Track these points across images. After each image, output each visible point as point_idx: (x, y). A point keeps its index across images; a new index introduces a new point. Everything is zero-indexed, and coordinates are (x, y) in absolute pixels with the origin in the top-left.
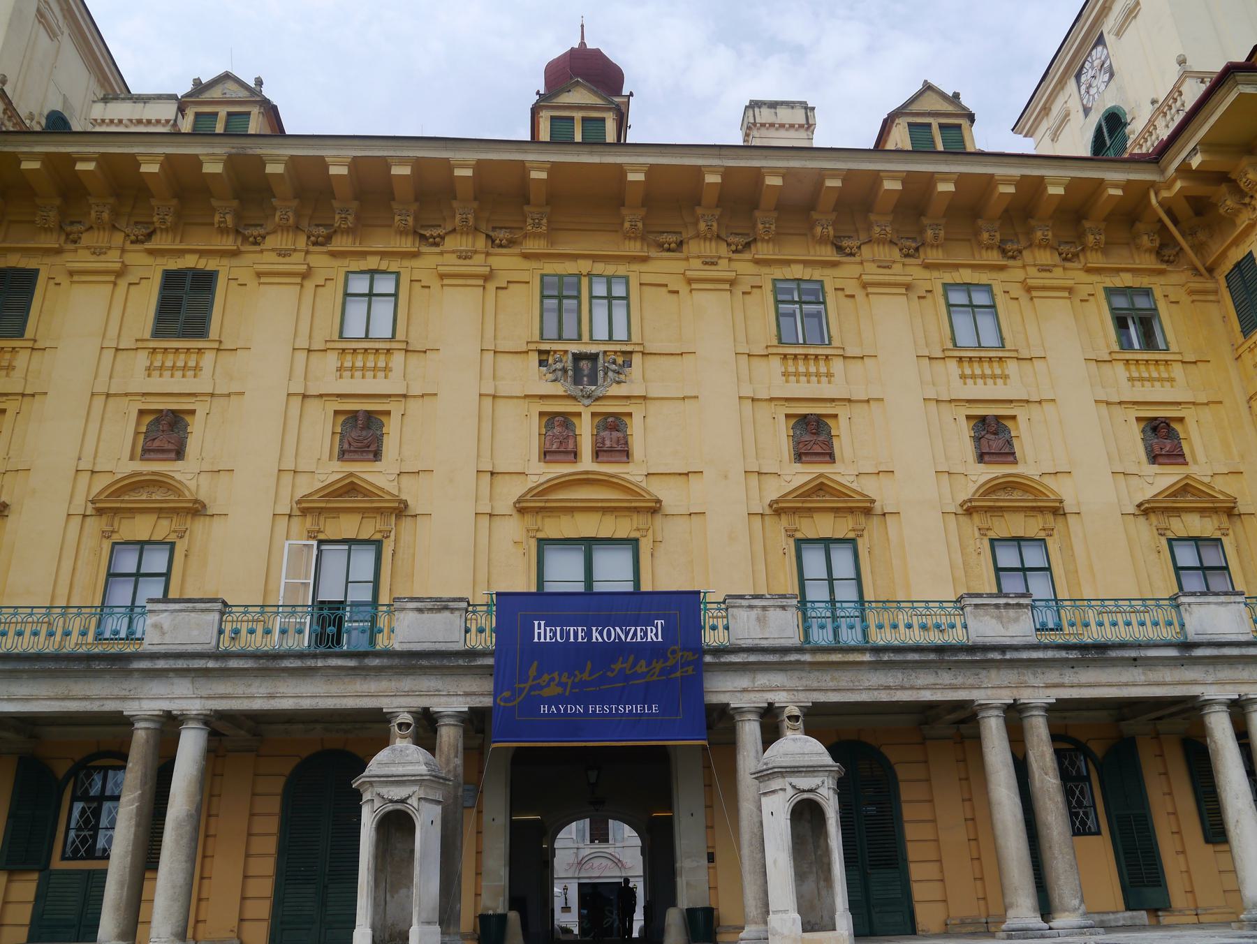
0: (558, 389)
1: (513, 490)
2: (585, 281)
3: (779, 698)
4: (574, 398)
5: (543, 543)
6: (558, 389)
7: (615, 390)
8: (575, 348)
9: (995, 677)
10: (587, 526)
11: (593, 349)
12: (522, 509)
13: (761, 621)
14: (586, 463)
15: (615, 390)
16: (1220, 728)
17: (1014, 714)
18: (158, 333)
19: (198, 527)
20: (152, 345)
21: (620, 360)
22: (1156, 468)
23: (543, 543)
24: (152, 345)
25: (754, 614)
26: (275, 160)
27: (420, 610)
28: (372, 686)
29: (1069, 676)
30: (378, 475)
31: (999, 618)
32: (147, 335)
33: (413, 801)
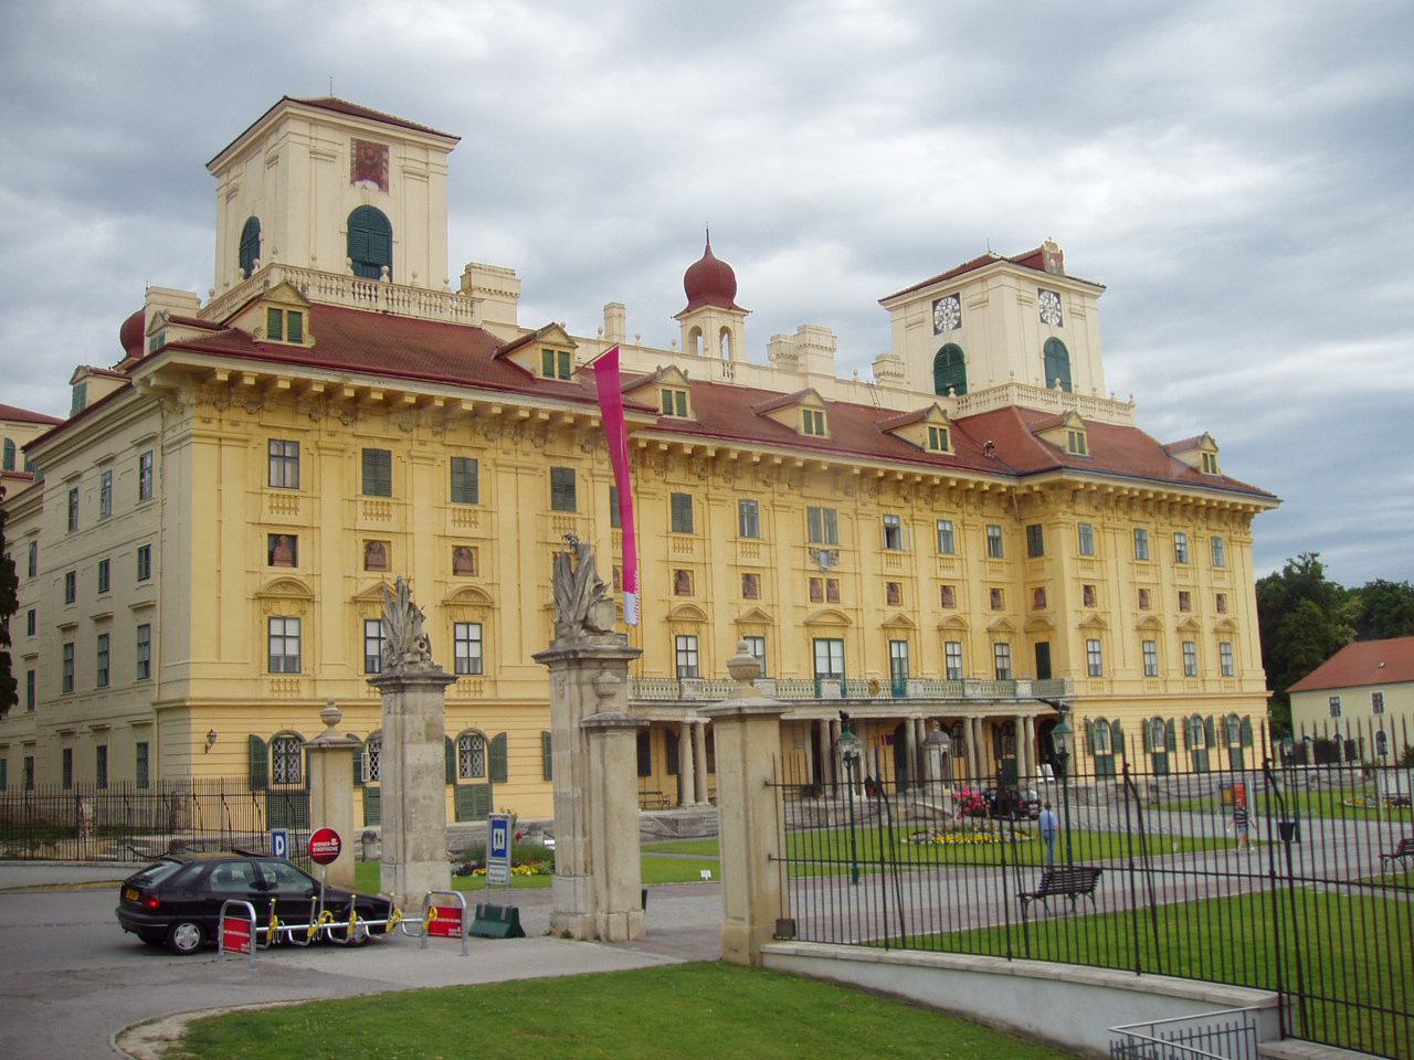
1: (803, 616)
3: (920, 715)
5: (815, 640)
6: (815, 567)
8: (821, 547)
9: (972, 708)
10: (830, 633)
11: (827, 548)
12: (808, 624)
15: (835, 569)
16: (1020, 724)
19: (703, 628)
22: (993, 612)
23: (815, 640)
26: (734, 451)
28: (821, 710)
29: (992, 708)
30: (760, 604)
32: (670, 530)
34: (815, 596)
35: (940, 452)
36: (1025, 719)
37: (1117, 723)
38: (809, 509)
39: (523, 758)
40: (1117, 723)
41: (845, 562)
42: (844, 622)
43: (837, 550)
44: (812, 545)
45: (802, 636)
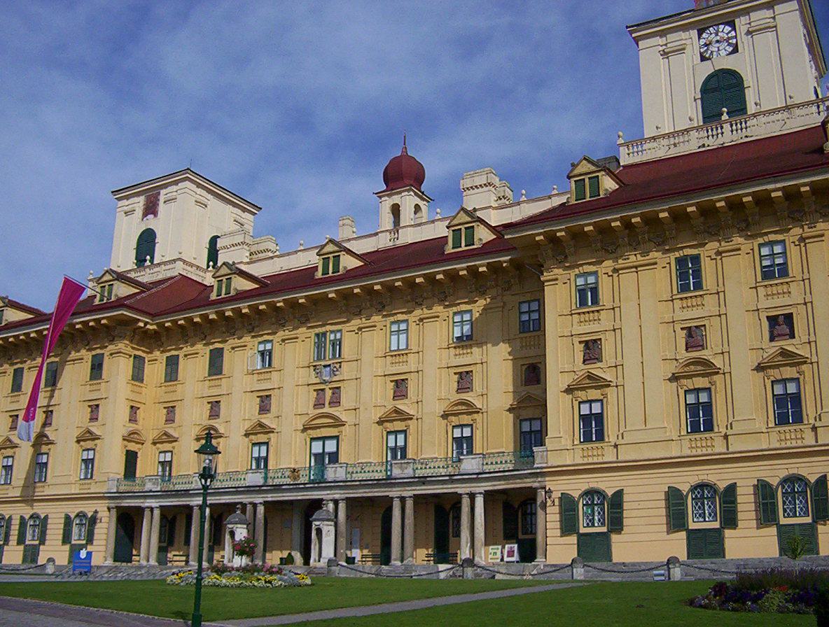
0: (318, 381)
2: (328, 334)
4: (321, 383)
5: (313, 439)
7: (335, 378)
8: (323, 363)
13: (335, 471)
14: (327, 409)
16: (466, 502)
17: (403, 499)
18: (210, 375)
20: (209, 378)
21: (338, 366)
24: (209, 378)
25: (333, 469)
27: (253, 473)
31: (401, 468)
32: (207, 375)
33: (234, 528)
34: (319, 404)
35: (464, 248)
36: (472, 496)
37: (619, 494)
38: (317, 335)
39: (55, 530)
40: (619, 494)
41: (346, 371)
42: (339, 423)
43: (340, 363)
44: (314, 364)
45: (300, 439)
